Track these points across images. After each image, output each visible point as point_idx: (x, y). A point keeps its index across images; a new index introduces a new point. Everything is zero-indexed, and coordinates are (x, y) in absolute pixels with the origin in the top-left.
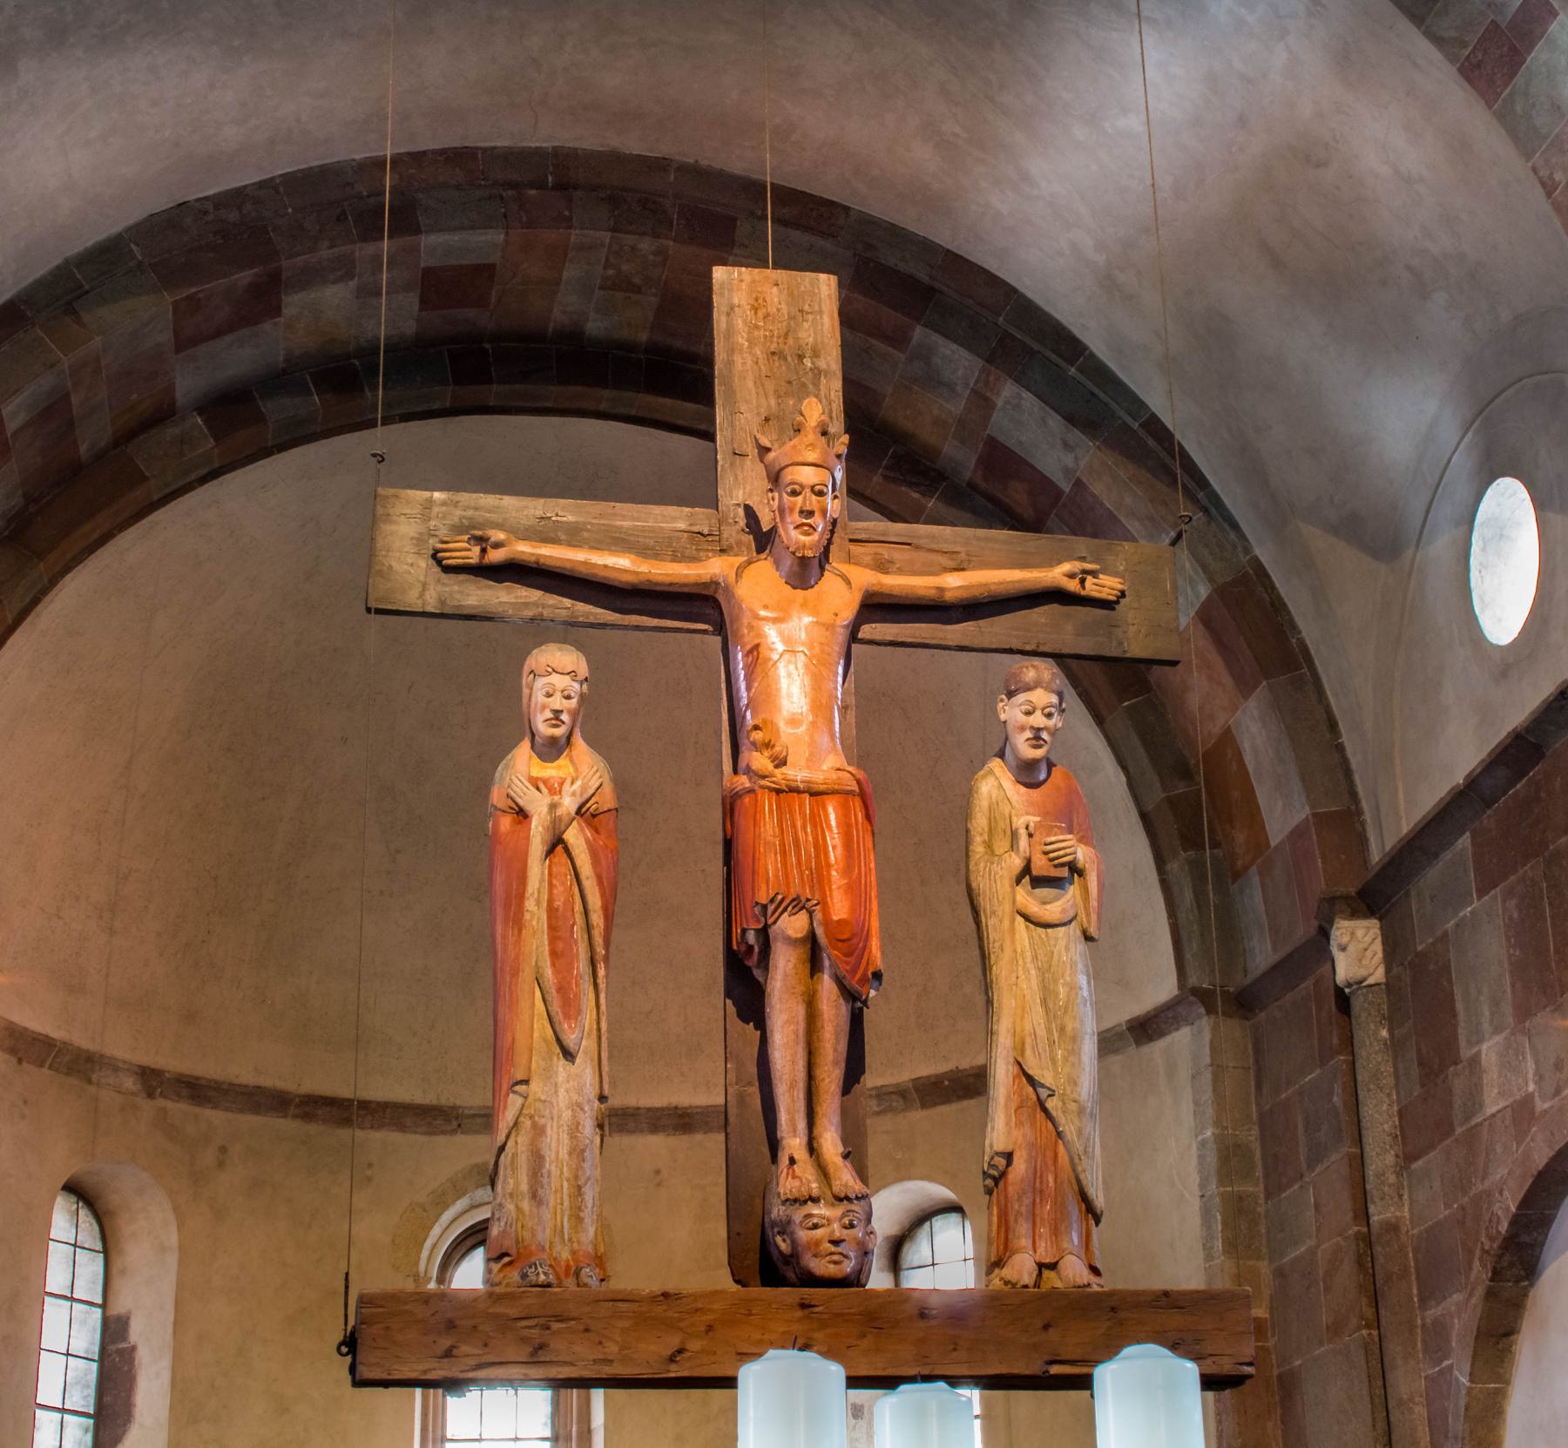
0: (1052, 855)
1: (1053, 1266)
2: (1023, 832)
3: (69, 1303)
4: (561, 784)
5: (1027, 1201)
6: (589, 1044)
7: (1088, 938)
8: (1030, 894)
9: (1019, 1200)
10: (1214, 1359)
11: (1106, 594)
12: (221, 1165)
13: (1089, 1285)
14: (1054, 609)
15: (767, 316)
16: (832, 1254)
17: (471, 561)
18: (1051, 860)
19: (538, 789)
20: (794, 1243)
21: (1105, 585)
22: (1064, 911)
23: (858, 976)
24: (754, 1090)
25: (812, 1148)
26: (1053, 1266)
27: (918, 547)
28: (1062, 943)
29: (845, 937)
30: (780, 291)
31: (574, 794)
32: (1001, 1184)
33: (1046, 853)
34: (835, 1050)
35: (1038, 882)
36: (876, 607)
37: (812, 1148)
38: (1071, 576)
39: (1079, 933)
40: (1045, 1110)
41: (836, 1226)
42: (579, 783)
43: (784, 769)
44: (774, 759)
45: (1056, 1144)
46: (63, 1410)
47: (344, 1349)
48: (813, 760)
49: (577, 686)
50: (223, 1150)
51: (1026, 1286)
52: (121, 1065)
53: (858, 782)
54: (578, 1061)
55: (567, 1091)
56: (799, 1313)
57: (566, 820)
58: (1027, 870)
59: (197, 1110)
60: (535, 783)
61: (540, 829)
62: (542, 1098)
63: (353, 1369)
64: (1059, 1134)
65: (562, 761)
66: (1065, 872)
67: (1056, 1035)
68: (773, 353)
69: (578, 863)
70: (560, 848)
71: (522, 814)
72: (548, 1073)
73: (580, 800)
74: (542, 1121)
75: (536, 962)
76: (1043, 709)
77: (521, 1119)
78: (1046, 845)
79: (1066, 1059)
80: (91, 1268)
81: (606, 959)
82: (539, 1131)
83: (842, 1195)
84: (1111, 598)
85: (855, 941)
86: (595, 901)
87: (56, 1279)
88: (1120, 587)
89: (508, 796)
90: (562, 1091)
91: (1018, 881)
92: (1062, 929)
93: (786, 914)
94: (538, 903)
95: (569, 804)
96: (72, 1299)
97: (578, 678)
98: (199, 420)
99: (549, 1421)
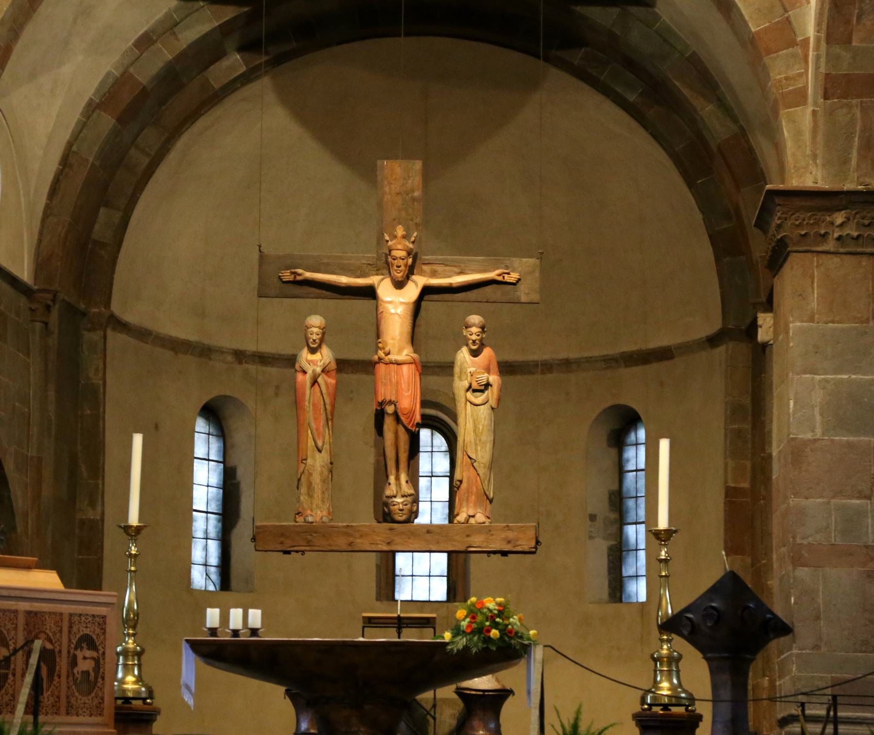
0: (479, 382)
1: (473, 516)
2: (469, 374)
3: (207, 462)
4: (317, 362)
5: (466, 495)
6: (327, 446)
7: (493, 409)
8: (472, 394)
9: (464, 494)
10: (522, 546)
11: (512, 280)
12: (277, 394)
13: (484, 523)
14: (494, 286)
15: (395, 179)
16: (400, 513)
17: (291, 279)
18: (478, 384)
19: (310, 364)
20: (389, 509)
21: (513, 277)
22: (483, 400)
23: (411, 425)
24: (382, 458)
25: (398, 478)
26: (473, 516)
27: (447, 265)
28: (482, 411)
29: (406, 413)
30: (401, 169)
31: (320, 366)
32: (459, 489)
33: (477, 381)
34: (404, 448)
35: (475, 391)
36: (427, 291)
37: (398, 478)
38: (499, 275)
39: (489, 407)
40: (473, 466)
41: (401, 505)
42: (322, 362)
43: (389, 356)
44: (384, 353)
45: (477, 477)
46: (207, 512)
47: (253, 540)
48: (400, 351)
49: (321, 331)
50: (277, 387)
51: (463, 523)
52: (224, 350)
53: (414, 359)
54: (323, 452)
55: (319, 462)
56: (388, 531)
57: (317, 375)
58: (470, 387)
59: (265, 368)
60: (309, 362)
61: (309, 378)
62: (311, 464)
63: (255, 547)
64: (478, 474)
65: (318, 354)
66: (483, 388)
67: (478, 442)
68: (398, 194)
69: (322, 389)
70: (316, 384)
71: (305, 372)
72: (313, 457)
73: (322, 368)
74: (311, 471)
75: (309, 421)
76: (475, 334)
77: (305, 471)
78: (477, 378)
79: (481, 450)
80: (215, 445)
81: (332, 420)
82: (311, 474)
83: (403, 495)
84: (515, 282)
85: (409, 414)
86: (328, 401)
87: (200, 450)
88: (518, 277)
89: (300, 367)
90: (317, 462)
91: (468, 390)
92: (482, 406)
93: (387, 406)
94: (309, 403)
95: (319, 370)
96: (209, 460)
97: (322, 328)
98: (238, 57)
99: (447, 517)
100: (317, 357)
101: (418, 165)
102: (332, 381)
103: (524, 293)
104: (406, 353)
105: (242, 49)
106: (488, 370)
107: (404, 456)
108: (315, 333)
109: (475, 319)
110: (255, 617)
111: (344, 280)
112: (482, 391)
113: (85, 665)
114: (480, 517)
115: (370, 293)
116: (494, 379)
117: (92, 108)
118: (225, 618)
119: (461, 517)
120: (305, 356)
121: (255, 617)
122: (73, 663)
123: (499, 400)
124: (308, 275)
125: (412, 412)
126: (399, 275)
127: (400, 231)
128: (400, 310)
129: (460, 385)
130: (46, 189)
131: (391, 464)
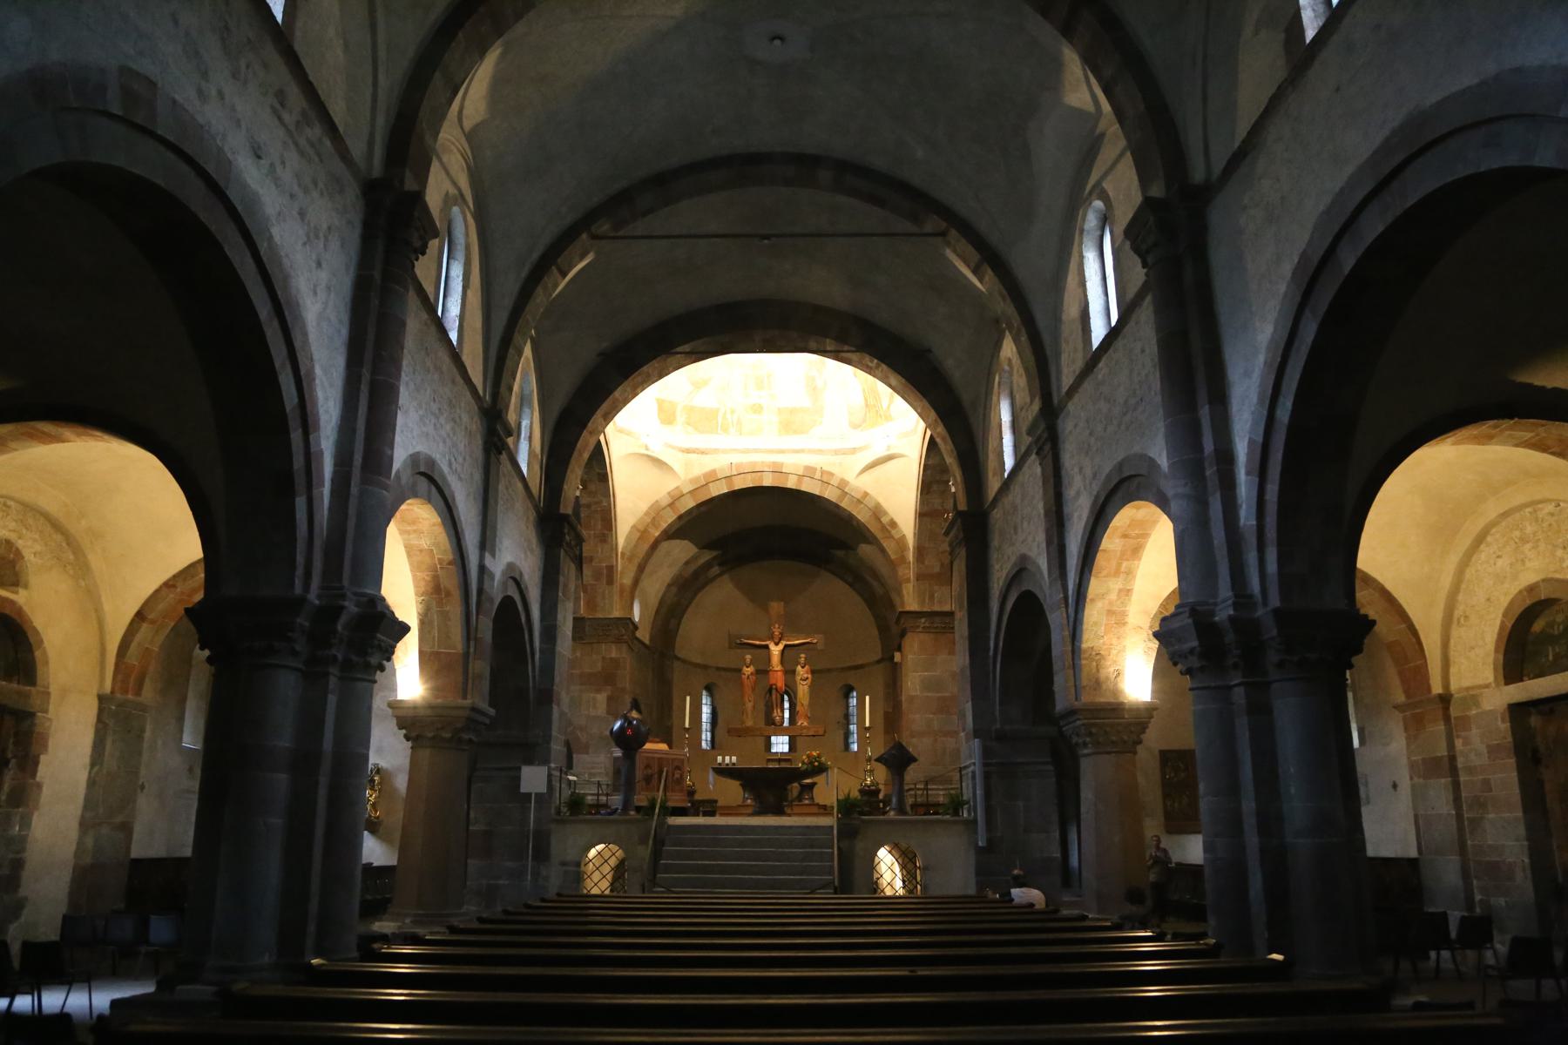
21: (815, 641)
36: (786, 646)
80: (709, 699)
87: (704, 701)
100: (749, 669)
101: (782, 603)
102: (754, 678)
103: (820, 647)
104: (779, 668)
105: (720, 565)
106: (807, 673)
107: (779, 701)
108: (748, 661)
109: (803, 655)
110: (734, 759)
111: (758, 643)
112: (805, 680)
113: (677, 776)
114: (805, 724)
115: (767, 647)
116: (810, 676)
117: (669, 586)
118: (724, 759)
119: (799, 724)
120: (745, 669)
121: (734, 759)
122: (673, 775)
123: (811, 683)
124: (746, 641)
125: (781, 688)
126: (777, 641)
127: (777, 626)
128: (777, 653)
129: (798, 678)
130: (654, 613)
131: (775, 706)
